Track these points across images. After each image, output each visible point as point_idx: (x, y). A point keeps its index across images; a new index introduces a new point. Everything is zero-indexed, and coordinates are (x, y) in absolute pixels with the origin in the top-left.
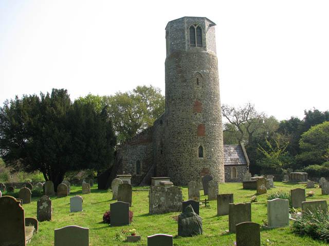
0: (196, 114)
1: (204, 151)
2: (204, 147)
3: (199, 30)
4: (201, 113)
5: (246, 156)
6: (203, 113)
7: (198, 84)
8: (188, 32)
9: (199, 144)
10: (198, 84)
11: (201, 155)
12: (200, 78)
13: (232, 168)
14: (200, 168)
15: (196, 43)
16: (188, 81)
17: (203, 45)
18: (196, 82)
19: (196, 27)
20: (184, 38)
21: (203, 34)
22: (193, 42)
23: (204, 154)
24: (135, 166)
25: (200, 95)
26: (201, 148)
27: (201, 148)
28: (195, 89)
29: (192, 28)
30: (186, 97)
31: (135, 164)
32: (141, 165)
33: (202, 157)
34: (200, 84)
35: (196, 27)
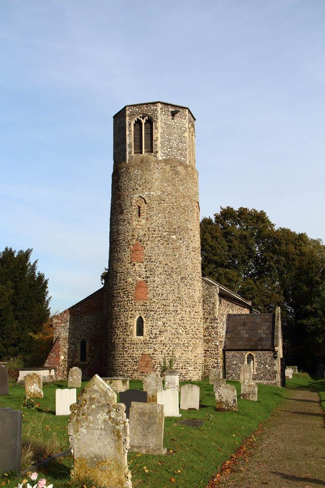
0: (134, 265)
1: (145, 324)
2: (144, 320)
3: (148, 125)
6: (145, 263)
7: (139, 215)
8: (130, 131)
10: (139, 215)
11: (140, 332)
12: (144, 207)
14: (137, 354)
17: (154, 150)
18: (136, 213)
19: (143, 121)
20: (125, 142)
21: (154, 131)
22: (139, 149)
23: (145, 330)
24: (79, 347)
25: (142, 233)
26: (140, 322)
27: (140, 322)
29: (138, 122)
31: (79, 343)
32: (87, 347)
33: (142, 335)
34: (144, 215)
35: (143, 121)
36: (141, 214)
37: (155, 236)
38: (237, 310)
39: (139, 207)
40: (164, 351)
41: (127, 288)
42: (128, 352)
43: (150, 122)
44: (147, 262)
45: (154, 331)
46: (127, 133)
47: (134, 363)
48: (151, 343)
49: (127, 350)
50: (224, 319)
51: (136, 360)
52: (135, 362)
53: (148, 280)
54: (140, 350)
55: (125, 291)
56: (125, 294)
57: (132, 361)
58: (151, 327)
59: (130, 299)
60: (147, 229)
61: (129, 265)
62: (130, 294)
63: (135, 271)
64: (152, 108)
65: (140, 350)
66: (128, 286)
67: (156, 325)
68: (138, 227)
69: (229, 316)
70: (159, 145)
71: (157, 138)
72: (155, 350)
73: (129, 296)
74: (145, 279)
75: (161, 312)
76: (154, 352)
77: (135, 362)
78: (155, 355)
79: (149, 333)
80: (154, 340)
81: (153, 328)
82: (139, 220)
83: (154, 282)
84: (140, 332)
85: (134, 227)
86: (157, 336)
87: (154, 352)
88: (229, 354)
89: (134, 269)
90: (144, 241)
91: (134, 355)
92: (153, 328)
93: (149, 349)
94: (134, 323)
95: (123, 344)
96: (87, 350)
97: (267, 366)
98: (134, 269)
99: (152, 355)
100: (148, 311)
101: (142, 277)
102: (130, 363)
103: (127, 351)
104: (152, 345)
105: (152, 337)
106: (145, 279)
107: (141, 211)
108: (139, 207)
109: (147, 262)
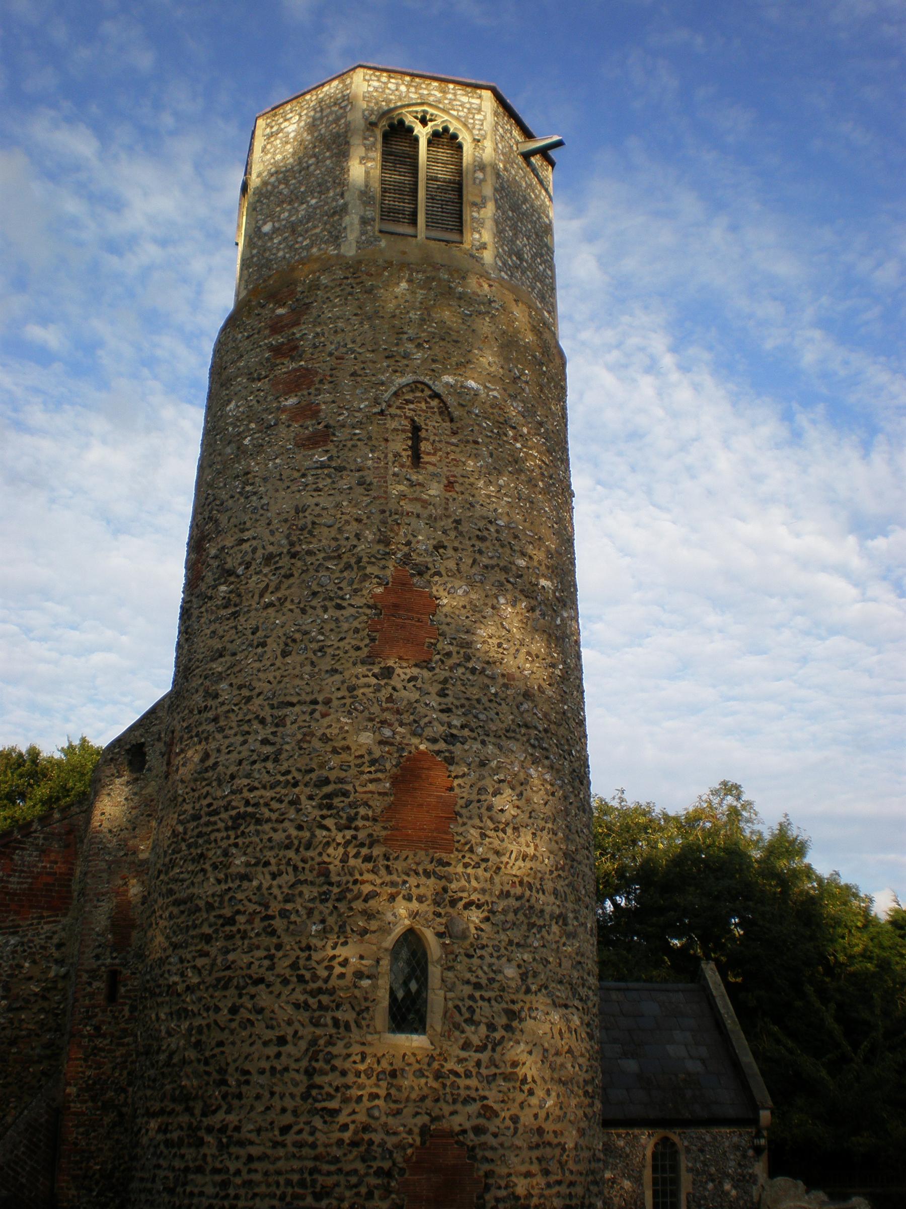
1: (435, 972)
4: (424, 664)
5: (747, 1058)
6: (443, 674)
7: (416, 458)
10: (416, 458)
16: (341, 435)
18: (400, 445)
28: (396, 489)
30: (324, 538)
36: (426, 458)
37: (485, 561)
39: (416, 429)
41: (341, 781)
42: (343, 1118)
44: (451, 669)
45: (484, 1011)
47: (373, 1181)
48: (468, 1075)
49: (333, 1104)
51: (386, 1165)
52: (379, 1172)
53: (458, 749)
54: (409, 1111)
55: (328, 796)
56: (330, 807)
57: (361, 1167)
58: (467, 990)
59: (362, 835)
60: (448, 523)
61: (361, 670)
62: (362, 811)
63: (390, 699)
64: (465, 99)
65: (409, 1111)
66: (353, 771)
67: (491, 980)
68: (408, 507)
73: (360, 823)
74: (441, 745)
75: (511, 917)
76: (481, 1121)
77: (379, 1172)
78: (488, 1139)
79: (458, 1018)
80: (484, 1057)
81: (477, 994)
82: (414, 478)
83: (483, 764)
85: (392, 505)
86: (497, 1036)
87: (481, 1121)
89: (384, 694)
90: (438, 574)
91: (377, 1138)
92: (477, 994)
93: (458, 1107)
95: (310, 1073)
97: (727, 1187)
98: (384, 694)
99: (471, 1139)
100: (453, 903)
101: (428, 732)
102: (354, 1180)
103: (334, 1113)
104: (473, 1082)
105: (476, 1041)
106: (441, 745)
107: (424, 446)
109: (451, 669)
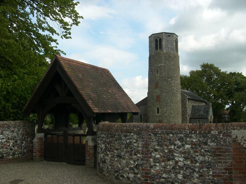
2: (159, 108)
8: (154, 43)
9: (157, 106)
11: (158, 112)
12: (159, 70)
13: (198, 120)
15: (159, 48)
19: (158, 39)
21: (162, 43)
23: (160, 112)
26: (158, 109)
27: (158, 109)
29: (156, 40)
32: (142, 117)
34: (159, 72)
35: (158, 39)
38: (197, 104)
40: (166, 119)
43: (160, 40)
45: (163, 112)
46: (153, 43)
50: (191, 107)
69: (193, 106)
70: (164, 47)
71: (163, 45)
72: (163, 119)
84: (158, 112)
88: (191, 119)
94: (156, 110)
96: (142, 118)
108: (157, 70)
